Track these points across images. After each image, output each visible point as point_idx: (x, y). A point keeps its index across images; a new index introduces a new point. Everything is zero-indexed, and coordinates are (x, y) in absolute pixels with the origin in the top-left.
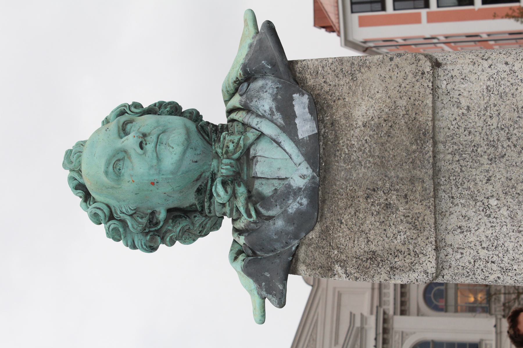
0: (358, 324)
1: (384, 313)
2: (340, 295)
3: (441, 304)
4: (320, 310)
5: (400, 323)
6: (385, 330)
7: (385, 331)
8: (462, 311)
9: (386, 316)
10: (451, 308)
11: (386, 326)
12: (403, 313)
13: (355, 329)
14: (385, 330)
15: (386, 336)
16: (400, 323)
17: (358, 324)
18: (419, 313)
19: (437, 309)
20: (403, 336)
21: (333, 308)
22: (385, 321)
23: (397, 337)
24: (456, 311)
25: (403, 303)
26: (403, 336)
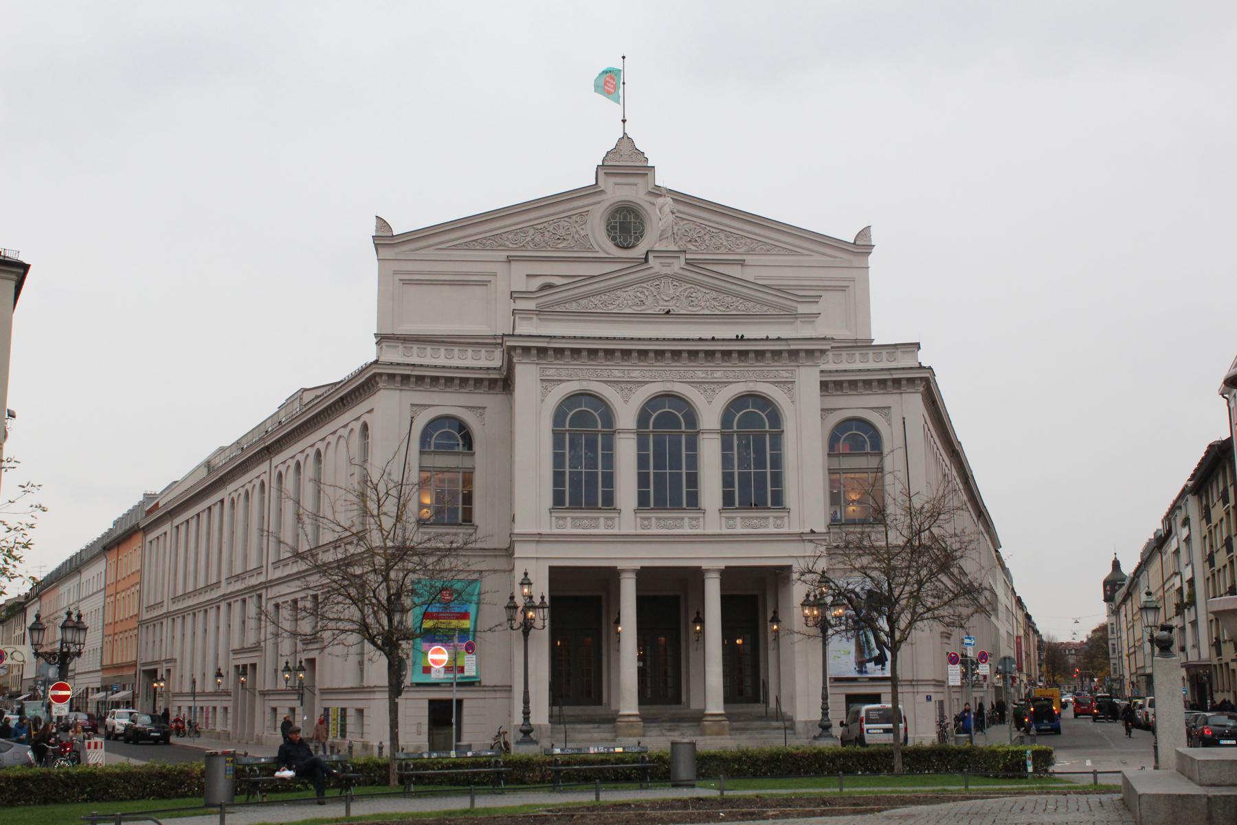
0: (803, 309)
1: (823, 352)
2: (843, 289)
3: (842, 447)
4: (817, 257)
5: (808, 378)
6: (795, 354)
7: (794, 354)
8: (832, 482)
9: (818, 354)
10: (835, 464)
11: (802, 354)
12: (824, 385)
13: (794, 304)
14: (795, 354)
15: (785, 355)
16: (808, 378)
17: (803, 309)
18: (825, 411)
19: (833, 440)
20: (787, 384)
21: (821, 279)
22: (810, 353)
23: (784, 374)
24: (831, 472)
25: (839, 385)
26: (787, 384)
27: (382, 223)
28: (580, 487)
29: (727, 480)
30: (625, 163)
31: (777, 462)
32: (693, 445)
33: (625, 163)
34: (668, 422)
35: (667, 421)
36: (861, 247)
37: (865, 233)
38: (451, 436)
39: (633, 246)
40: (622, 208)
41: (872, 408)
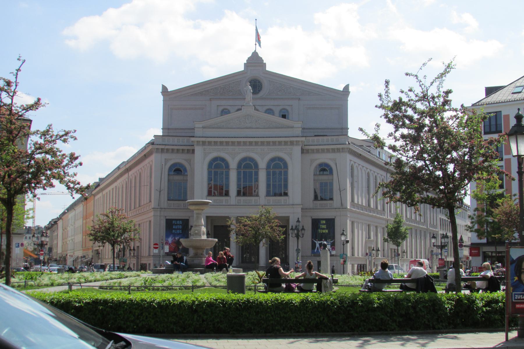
16: (297, 150)
27: (164, 88)
28: (218, 189)
29: (268, 186)
30: (255, 61)
31: (286, 180)
32: (257, 174)
33: (255, 61)
34: (248, 166)
35: (248, 166)
36: (346, 91)
37: (347, 88)
38: (178, 170)
39: (258, 93)
40: (255, 79)
41: (330, 159)
